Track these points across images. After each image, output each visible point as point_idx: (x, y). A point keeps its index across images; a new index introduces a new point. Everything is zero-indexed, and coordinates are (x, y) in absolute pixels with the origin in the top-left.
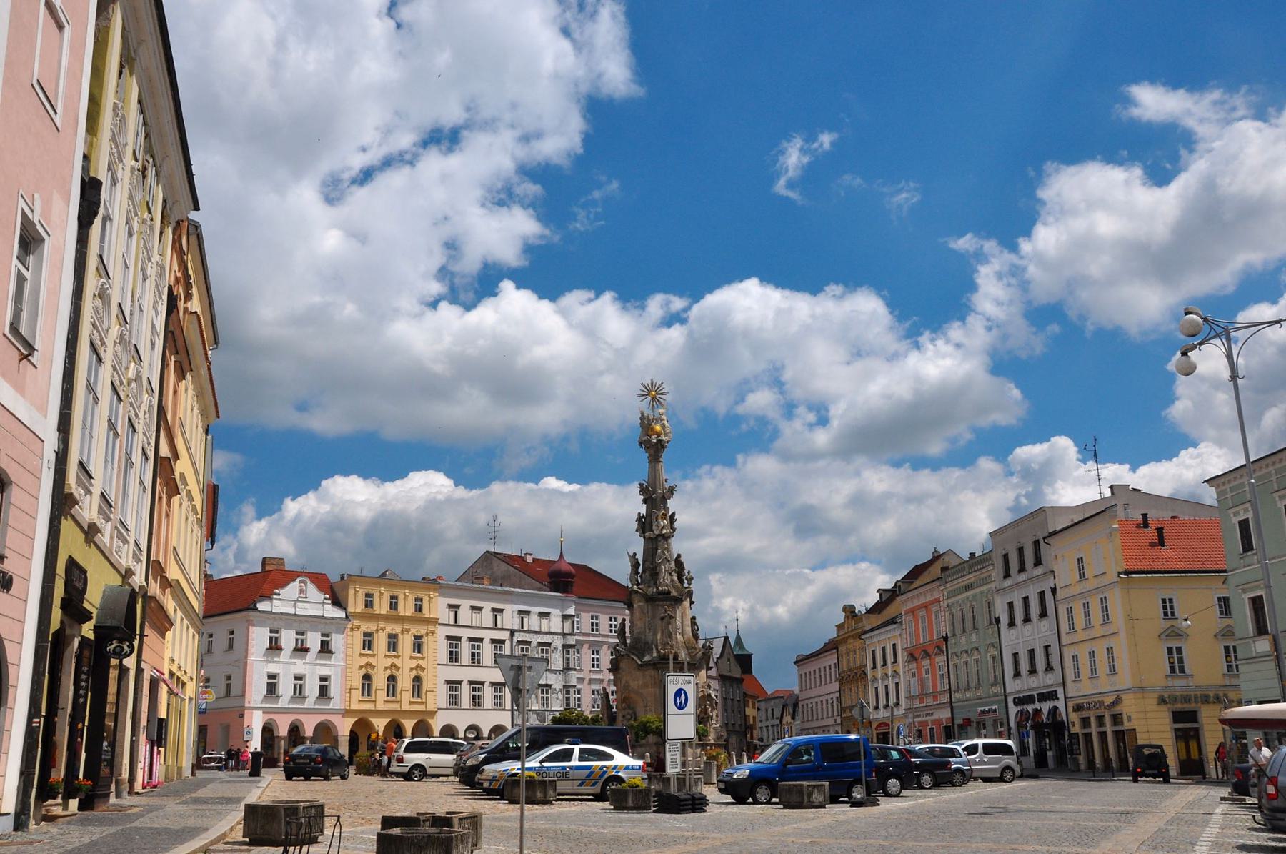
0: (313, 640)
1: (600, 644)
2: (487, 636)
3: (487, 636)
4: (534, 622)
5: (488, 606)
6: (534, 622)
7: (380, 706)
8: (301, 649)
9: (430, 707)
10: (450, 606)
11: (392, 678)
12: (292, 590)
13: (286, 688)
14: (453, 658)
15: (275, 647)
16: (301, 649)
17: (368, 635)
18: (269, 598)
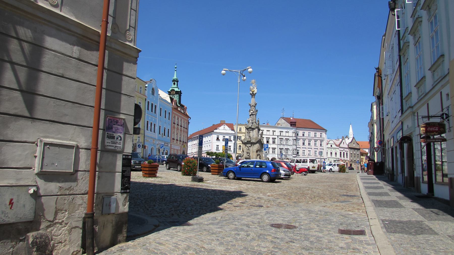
1: (317, 140)
2: (271, 137)
3: (271, 137)
4: (284, 134)
5: (271, 130)
6: (284, 134)
12: (222, 127)
15: (218, 139)
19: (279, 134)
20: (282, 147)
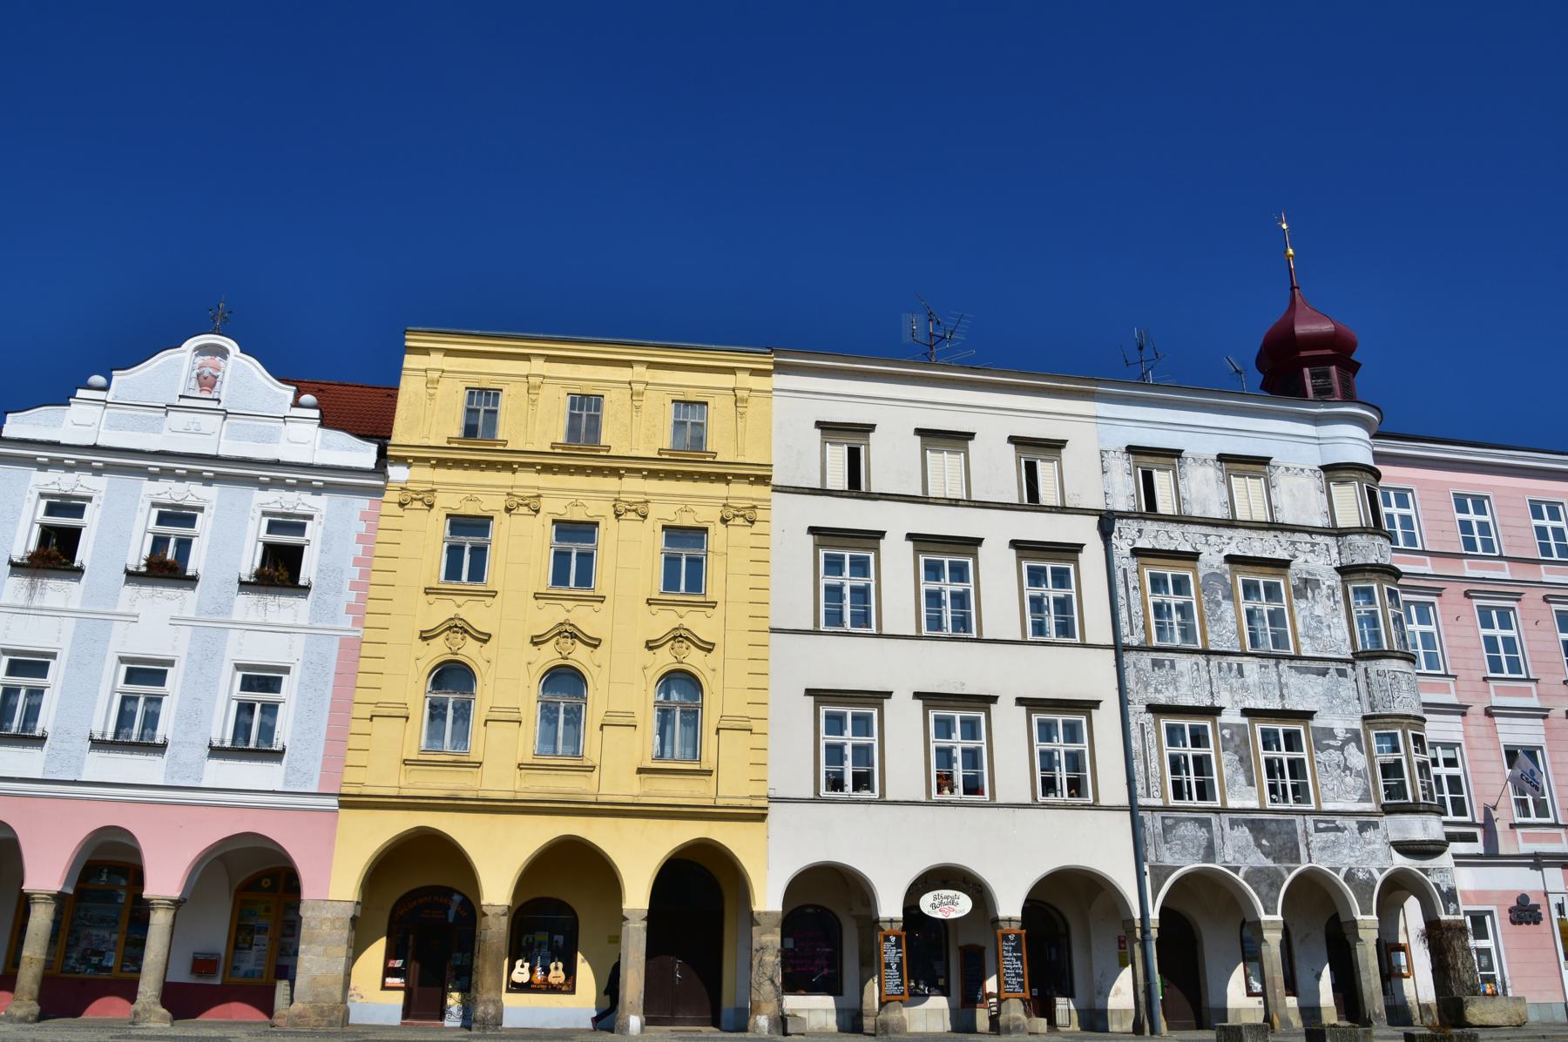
4: (1202, 489)
7: (499, 780)
8: (165, 569)
9: (733, 787)
10: (828, 429)
11: (564, 682)
14: (845, 611)
16: (165, 569)
19: (1123, 493)
20: (1187, 683)
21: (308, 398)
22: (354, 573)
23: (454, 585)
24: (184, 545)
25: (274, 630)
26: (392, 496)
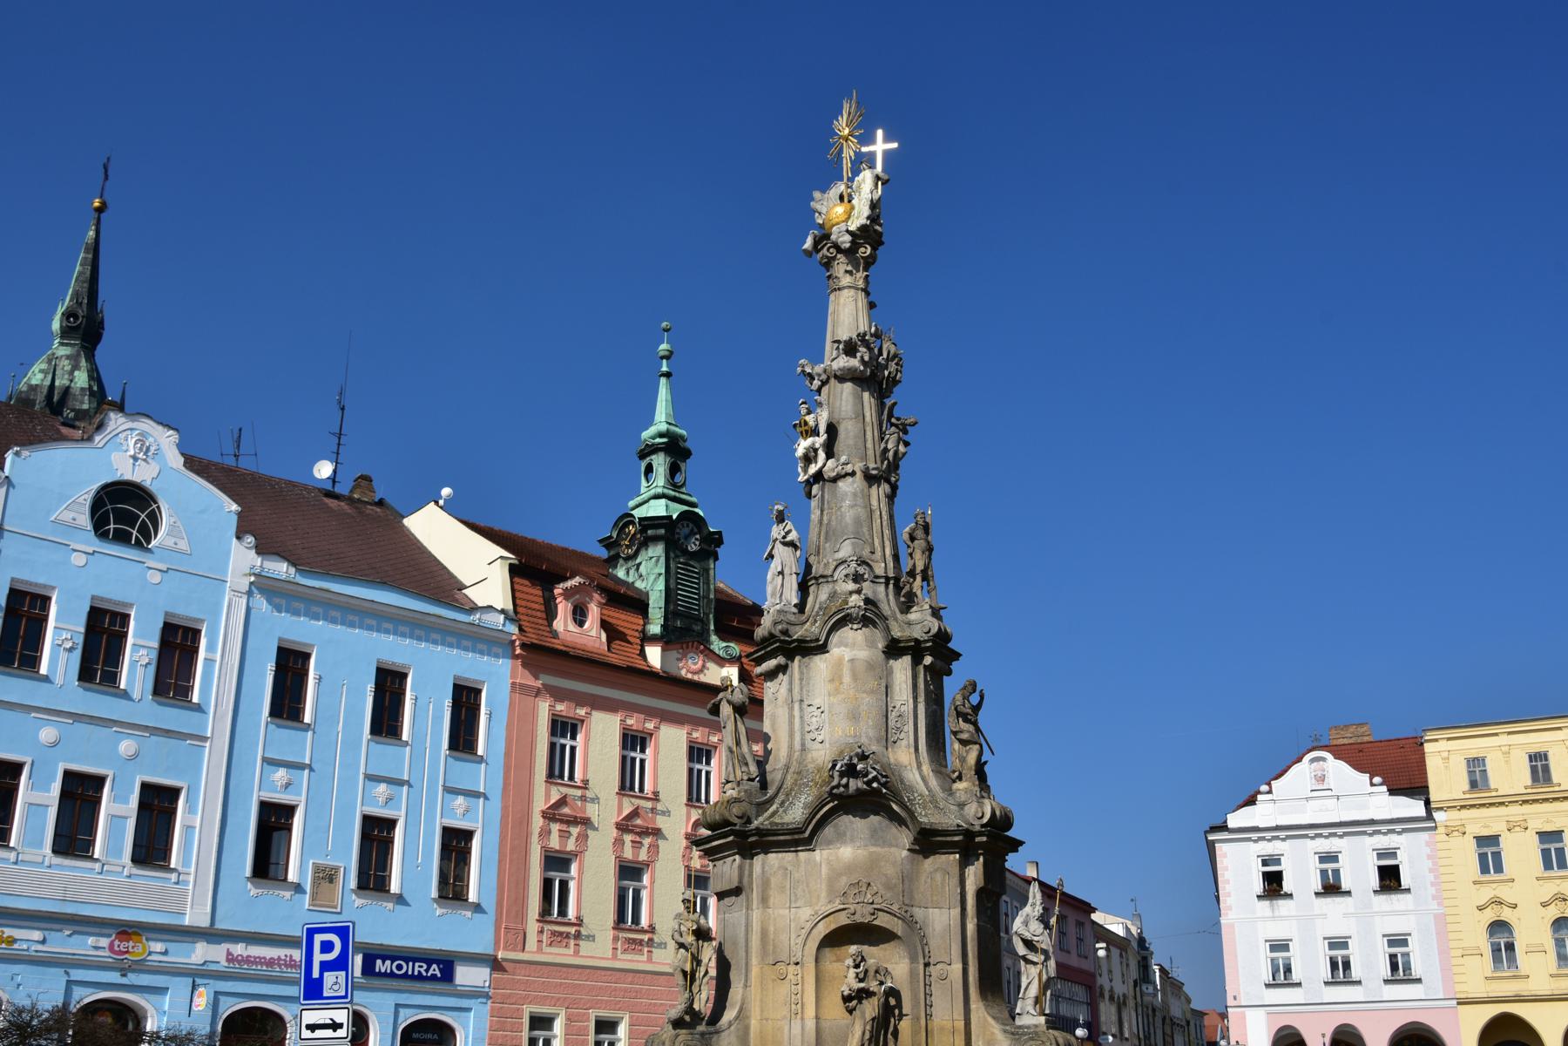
0: (1359, 869)
12: (1300, 775)
13: (1310, 964)
15: (1273, 884)
16: (1331, 888)
17: (1487, 842)
18: (1251, 801)
21: (1377, 780)
22: (1431, 877)
23: (1486, 878)
24: (1336, 872)
25: (1394, 913)
26: (1441, 830)
